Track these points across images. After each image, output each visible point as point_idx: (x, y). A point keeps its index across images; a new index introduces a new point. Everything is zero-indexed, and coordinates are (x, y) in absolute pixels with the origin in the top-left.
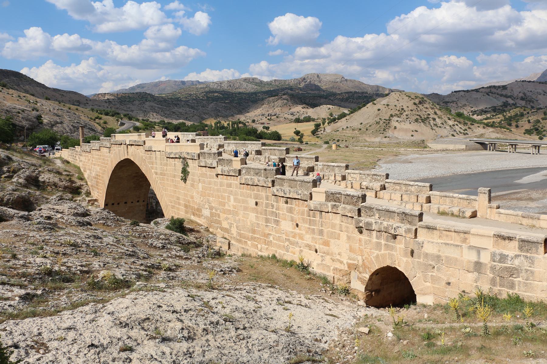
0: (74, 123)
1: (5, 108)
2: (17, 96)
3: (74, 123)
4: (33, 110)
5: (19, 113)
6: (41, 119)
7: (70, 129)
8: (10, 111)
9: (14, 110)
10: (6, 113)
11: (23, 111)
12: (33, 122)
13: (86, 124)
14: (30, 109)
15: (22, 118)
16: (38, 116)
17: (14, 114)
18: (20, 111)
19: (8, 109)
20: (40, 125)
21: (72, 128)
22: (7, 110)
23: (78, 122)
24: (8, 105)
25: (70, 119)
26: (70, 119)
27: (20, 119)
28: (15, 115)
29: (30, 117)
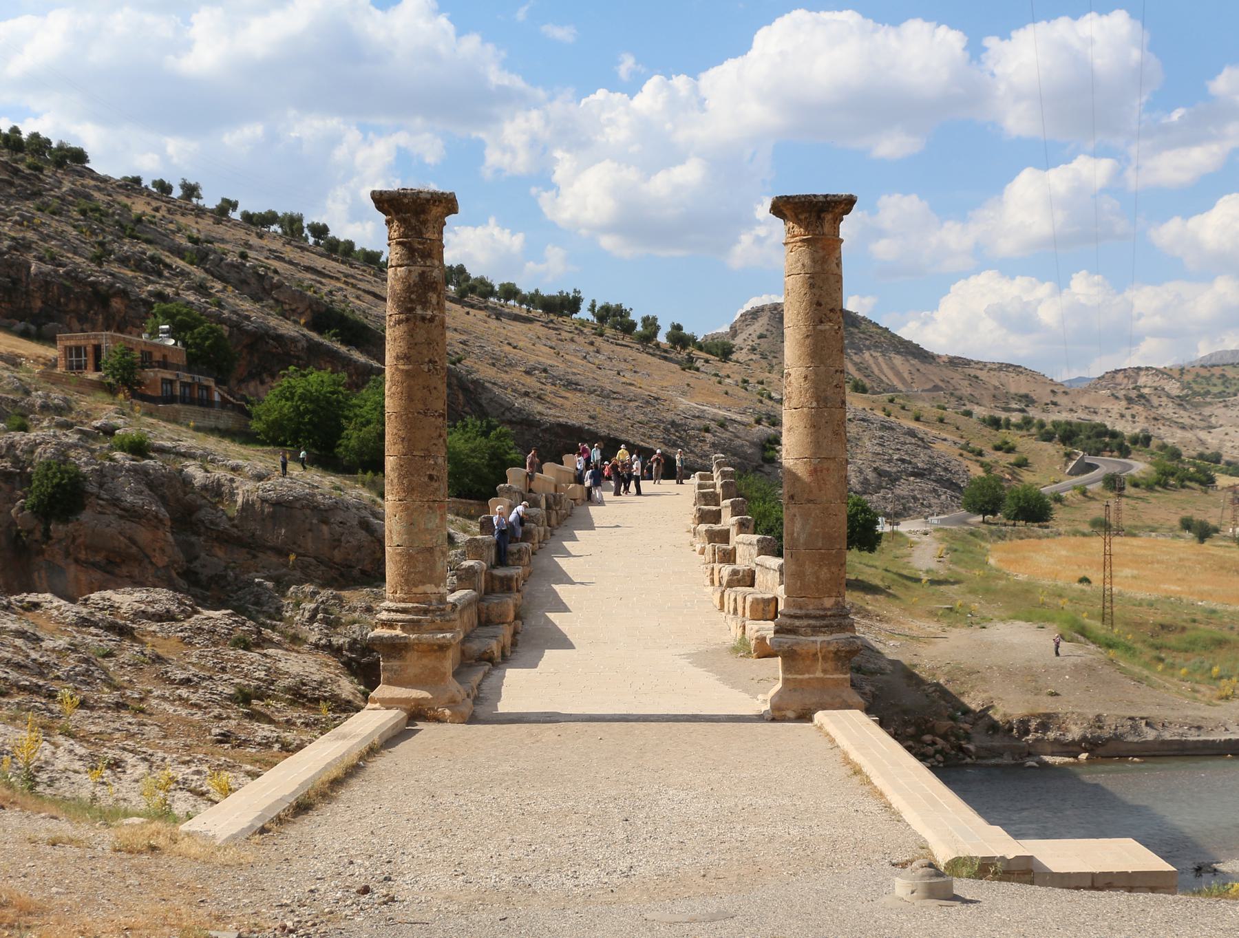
0: (890, 461)
1: (669, 416)
2: (740, 380)
3: (890, 461)
4: (758, 422)
5: (707, 430)
6: (774, 449)
7: (865, 482)
8: (681, 425)
9: (697, 421)
10: (666, 430)
11: (722, 425)
12: (745, 457)
13: (937, 465)
14: (752, 420)
15: (713, 445)
16: (769, 441)
17: (691, 433)
18: (713, 425)
19: (677, 419)
20: (767, 468)
21: (871, 476)
22: (673, 423)
23: (903, 461)
24: (681, 407)
25: (879, 449)
26: (879, 449)
27: (706, 448)
28: (693, 437)
29: (738, 442)
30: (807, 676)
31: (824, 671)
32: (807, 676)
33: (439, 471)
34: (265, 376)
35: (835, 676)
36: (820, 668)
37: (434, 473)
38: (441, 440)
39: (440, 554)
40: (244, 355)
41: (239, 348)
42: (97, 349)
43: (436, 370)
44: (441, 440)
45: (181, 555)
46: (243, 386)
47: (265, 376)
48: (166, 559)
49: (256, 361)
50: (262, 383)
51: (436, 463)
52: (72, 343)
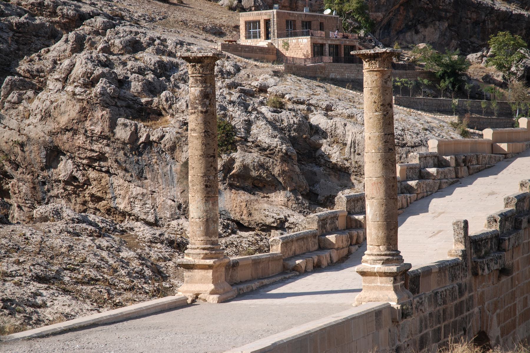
30: (373, 285)
31: (381, 283)
32: (373, 285)
33: (210, 183)
34: (419, 27)
35: (386, 285)
36: (379, 280)
37: (209, 184)
38: (212, 168)
39: (212, 222)
40: (401, 11)
41: (397, 6)
42: (267, 22)
43: (209, 135)
44: (212, 168)
45: (305, 182)
46: (401, 37)
47: (419, 27)
48: (294, 185)
49: (411, 16)
50: (417, 32)
51: (209, 179)
52: (251, 18)
